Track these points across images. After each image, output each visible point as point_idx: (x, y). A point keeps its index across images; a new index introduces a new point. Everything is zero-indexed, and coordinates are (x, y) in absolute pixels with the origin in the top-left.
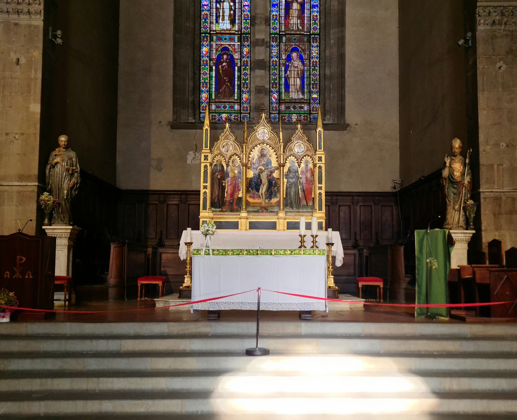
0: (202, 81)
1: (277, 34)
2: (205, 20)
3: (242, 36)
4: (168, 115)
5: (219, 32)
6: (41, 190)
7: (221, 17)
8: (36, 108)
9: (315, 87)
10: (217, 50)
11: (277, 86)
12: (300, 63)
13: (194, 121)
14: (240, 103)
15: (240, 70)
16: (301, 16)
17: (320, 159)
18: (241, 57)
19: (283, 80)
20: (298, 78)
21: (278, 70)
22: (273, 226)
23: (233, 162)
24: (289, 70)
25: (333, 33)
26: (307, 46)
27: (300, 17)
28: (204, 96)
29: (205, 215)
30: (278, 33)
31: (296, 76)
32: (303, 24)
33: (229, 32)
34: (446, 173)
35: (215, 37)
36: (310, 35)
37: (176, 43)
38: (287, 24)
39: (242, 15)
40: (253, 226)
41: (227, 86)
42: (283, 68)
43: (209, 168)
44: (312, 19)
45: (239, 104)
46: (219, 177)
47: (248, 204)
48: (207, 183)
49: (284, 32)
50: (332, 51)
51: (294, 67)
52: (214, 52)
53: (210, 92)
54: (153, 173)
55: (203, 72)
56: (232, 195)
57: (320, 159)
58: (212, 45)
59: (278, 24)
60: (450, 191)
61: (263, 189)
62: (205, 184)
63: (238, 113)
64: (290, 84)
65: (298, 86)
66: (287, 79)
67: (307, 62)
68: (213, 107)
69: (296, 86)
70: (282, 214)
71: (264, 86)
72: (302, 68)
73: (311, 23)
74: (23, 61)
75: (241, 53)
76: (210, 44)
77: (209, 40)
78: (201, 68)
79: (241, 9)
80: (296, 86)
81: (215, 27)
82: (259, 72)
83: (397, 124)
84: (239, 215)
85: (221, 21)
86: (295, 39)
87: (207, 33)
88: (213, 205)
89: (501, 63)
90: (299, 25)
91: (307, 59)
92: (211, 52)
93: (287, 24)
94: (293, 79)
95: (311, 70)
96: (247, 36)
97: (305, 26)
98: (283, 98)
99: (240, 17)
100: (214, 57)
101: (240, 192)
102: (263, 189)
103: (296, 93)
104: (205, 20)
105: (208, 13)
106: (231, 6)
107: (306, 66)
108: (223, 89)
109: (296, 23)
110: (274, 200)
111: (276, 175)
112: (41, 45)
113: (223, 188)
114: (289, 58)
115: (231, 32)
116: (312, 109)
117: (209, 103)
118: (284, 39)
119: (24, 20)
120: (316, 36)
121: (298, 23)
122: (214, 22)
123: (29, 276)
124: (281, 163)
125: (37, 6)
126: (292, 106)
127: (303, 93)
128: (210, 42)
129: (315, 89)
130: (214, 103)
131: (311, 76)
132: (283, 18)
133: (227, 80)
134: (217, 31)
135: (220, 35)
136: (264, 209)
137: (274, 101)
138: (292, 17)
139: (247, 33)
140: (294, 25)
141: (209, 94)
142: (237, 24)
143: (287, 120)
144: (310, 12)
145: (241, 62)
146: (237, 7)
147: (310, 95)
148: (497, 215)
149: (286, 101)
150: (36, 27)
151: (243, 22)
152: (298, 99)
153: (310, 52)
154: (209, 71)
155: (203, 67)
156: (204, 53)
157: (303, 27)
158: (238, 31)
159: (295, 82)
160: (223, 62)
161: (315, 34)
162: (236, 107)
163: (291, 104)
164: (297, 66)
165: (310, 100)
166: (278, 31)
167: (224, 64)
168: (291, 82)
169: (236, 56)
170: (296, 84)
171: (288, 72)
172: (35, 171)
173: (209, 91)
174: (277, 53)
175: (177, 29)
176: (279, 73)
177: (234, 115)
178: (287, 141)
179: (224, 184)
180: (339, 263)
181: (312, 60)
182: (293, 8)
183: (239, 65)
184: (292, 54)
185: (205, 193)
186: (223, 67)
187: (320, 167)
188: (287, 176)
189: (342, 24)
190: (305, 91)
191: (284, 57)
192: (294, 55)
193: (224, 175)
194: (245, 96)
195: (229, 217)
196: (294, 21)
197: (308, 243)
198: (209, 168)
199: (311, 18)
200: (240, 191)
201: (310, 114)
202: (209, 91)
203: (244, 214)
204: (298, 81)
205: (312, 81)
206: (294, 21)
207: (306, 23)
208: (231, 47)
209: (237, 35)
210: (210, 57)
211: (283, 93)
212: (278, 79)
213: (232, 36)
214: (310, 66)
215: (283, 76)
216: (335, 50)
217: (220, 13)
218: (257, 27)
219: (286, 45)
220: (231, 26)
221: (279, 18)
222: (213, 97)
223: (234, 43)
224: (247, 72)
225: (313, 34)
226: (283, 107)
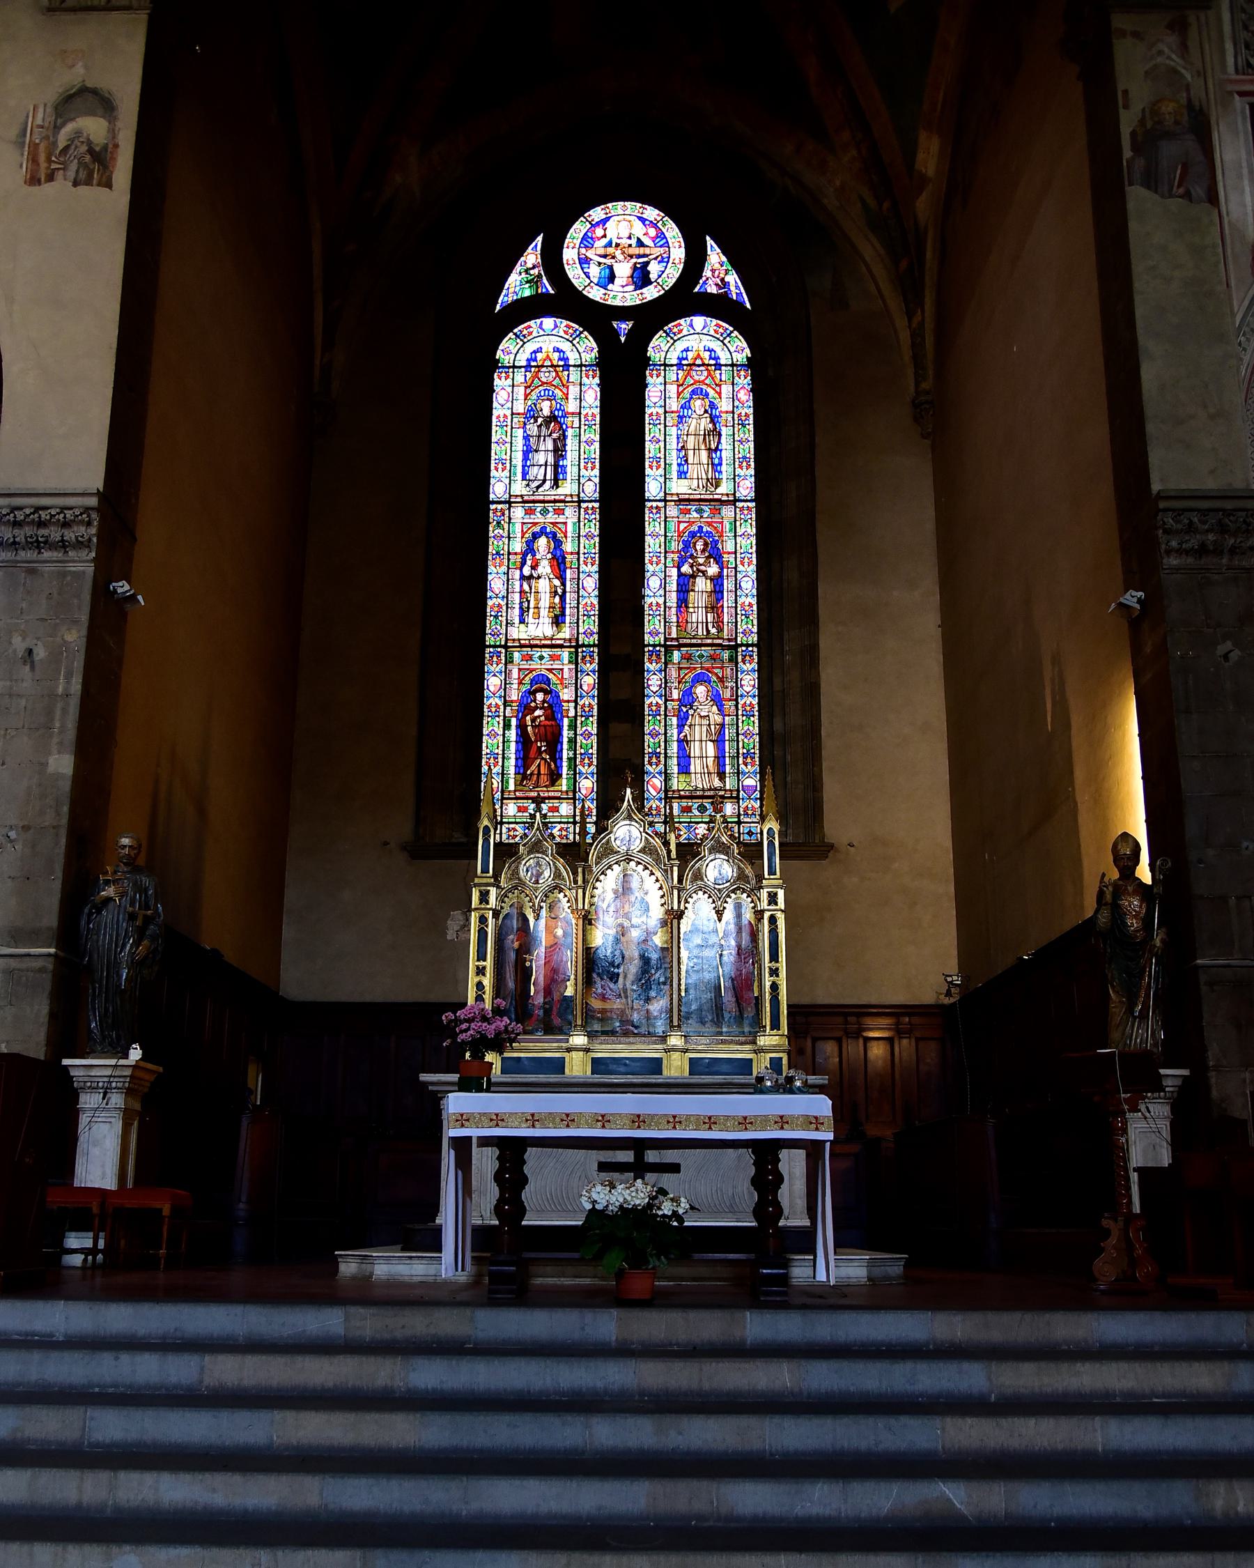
0: (485, 751)
1: (660, 645)
2: (496, 617)
3: (580, 650)
5: (527, 642)
7: (531, 611)
9: (749, 760)
10: (520, 683)
11: (659, 761)
12: (715, 708)
13: (463, 840)
15: (573, 727)
16: (715, 607)
17: (773, 899)
19: (675, 746)
20: (710, 741)
21: (663, 724)
23: (551, 908)
24: (688, 723)
26: (729, 669)
27: (712, 608)
30: (662, 642)
31: (704, 738)
32: (719, 624)
33: (549, 642)
35: (517, 656)
36: (737, 646)
39: (581, 606)
41: (543, 762)
42: (675, 720)
43: (491, 921)
44: (739, 612)
45: (572, 801)
46: (516, 945)
47: (588, 1014)
48: (485, 960)
49: (677, 639)
51: (701, 717)
52: (515, 686)
55: (487, 732)
56: (548, 991)
57: (773, 899)
58: (510, 671)
59: (662, 624)
62: (482, 963)
63: (568, 823)
64: (692, 755)
65: (710, 761)
66: (683, 742)
67: (729, 706)
69: (705, 759)
71: (630, 759)
72: (719, 719)
73: (739, 620)
75: (577, 687)
76: (506, 668)
77: (503, 661)
78: (485, 722)
79: (578, 593)
80: (705, 759)
81: (518, 632)
83: (948, 843)
84: (567, 1041)
85: (530, 619)
86: (701, 656)
87: (500, 646)
90: (710, 626)
91: (730, 700)
92: (507, 686)
94: (697, 743)
95: (740, 724)
96: (592, 649)
97: (725, 627)
98: (675, 788)
99: (576, 610)
100: (514, 695)
101: (568, 983)
103: (706, 775)
104: (496, 617)
105: (503, 603)
106: (556, 587)
107: (729, 715)
108: (533, 767)
109: (704, 621)
114: (688, 699)
115: (553, 642)
116: (744, 811)
118: (676, 656)
120: (750, 649)
121: (709, 621)
122: (517, 620)
124: (672, 908)
125: (83, 529)
126: (695, 804)
127: (722, 776)
128: (506, 664)
129: (749, 767)
130: (514, 801)
131: (741, 737)
132: (674, 611)
133: (543, 749)
134: (522, 642)
135: (529, 649)
137: (654, 793)
138: (694, 608)
139: (592, 643)
140: (700, 625)
141: (502, 781)
142: (567, 625)
143: (685, 839)
144: (736, 596)
145: (576, 708)
146: (568, 589)
147: (739, 780)
149: (682, 793)
150: (79, 575)
151: (581, 621)
152: (710, 789)
153: (736, 683)
154: (501, 730)
155: (490, 719)
156: (492, 689)
157: (720, 630)
158: (570, 640)
159: (703, 752)
160: (536, 708)
161: (747, 645)
163: (694, 801)
164: (708, 716)
165: (738, 791)
166: (662, 639)
167: (538, 713)
168: (695, 750)
169: (566, 694)
170: (704, 755)
171: (686, 727)
173: (503, 774)
174: (660, 686)
176: (666, 730)
177: (559, 827)
179: (528, 964)
181: (741, 702)
182: (696, 590)
183: (572, 713)
184: (696, 687)
185: (480, 986)
186: (533, 720)
187: (773, 920)
190: (727, 771)
191: (675, 695)
192: (700, 690)
196: (698, 616)
198: (491, 921)
199: (739, 609)
200: (569, 980)
201: (739, 823)
202: (503, 774)
203: (579, 1040)
204: (711, 749)
205: (743, 748)
206: (698, 616)
207: (725, 620)
208: (555, 674)
209: (569, 650)
210: (505, 697)
211: (676, 775)
212: (662, 744)
213: (557, 651)
214: (737, 715)
215: (675, 738)
217: (529, 602)
219: (680, 669)
220: (555, 628)
221: (665, 611)
222: (512, 787)
223: (561, 667)
224: (589, 729)
225: (742, 645)
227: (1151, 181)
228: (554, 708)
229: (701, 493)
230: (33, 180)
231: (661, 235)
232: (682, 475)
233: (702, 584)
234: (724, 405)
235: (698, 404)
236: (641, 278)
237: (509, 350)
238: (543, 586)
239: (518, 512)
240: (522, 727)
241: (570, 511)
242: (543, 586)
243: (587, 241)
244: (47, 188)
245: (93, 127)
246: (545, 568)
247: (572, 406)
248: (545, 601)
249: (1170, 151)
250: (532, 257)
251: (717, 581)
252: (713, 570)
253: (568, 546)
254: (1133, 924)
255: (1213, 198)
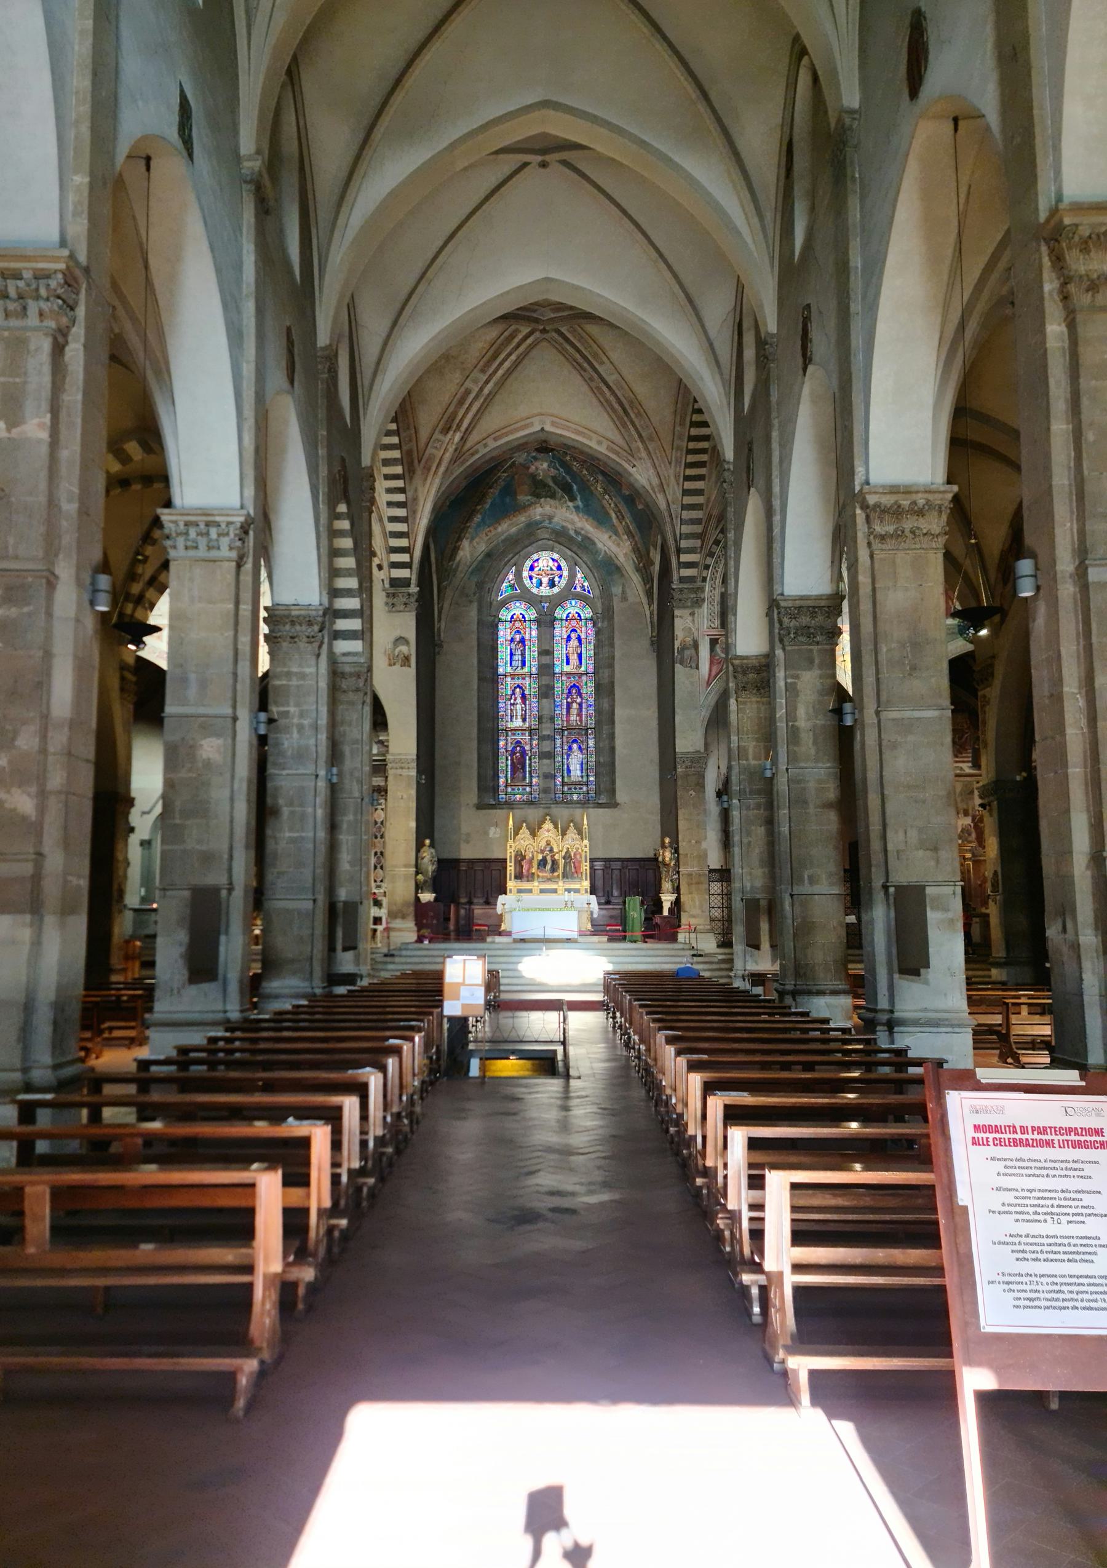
4: (475, 800)
6: (417, 873)
8: (413, 824)
14: (531, 786)
15: (530, 759)
16: (579, 714)
18: (531, 748)
22: (555, 891)
25: (606, 729)
28: (502, 781)
29: (511, 884)
32: (581, 720)
34: (660, 859)
37: (480, 741)
38: (568, 721)
40: (542, 891)
50: (605, 744)
53: (506, 777)
54: (463, 846)
56: (528, 870)
60: (663, 870)
61: (549, 867)
68: (509, 789)
70: (561, 883)
74: (405, 796)
82: (546, 761)
88: (516, 877)
89: (692, 792)
93: (568, 721)
100: (510, 749)
102: (549, 867)
110: (556, 874)
111: (556, 857)
112: (415, 786)
113: (522, 867)
114: (570, 748)
117: (506, 786)
119: (405, 772)
123: (435, 922)
136: (549, 880)
148: (689, 884)
162: (528, 789)
168: (572, 768)
169: (527, 748)
172: (413, 862)
175: (480, 730)
178: (564, 834)
180: (595, 916)
188: (564, 858)
189: (612, 722)
193: (524, 858)
194: (535, 780)
195: (526, 885)
196: (574, 718)
197: (569, 905)
204: (578, 767)
206: (574, 718)
216: (607, 742)
218: (544, 725)
226: (566, 788)
227: (681, 664)
228: (523, 753)
229: (575, 671)
230: (390, 665)
231: (559, 568)
232: (568, 663)
233: (575, 706)
234: (583, 636)
235: (573, 635)
236: (552, 584)
237: (504, 614)
238: (519, 707)
239: (509, 679)
240: (512, 760)
241: (527, 679)
242: (519, 707)
243: (532, 568)
244: (394, 667)
245: (404, 649)
246: (519, 700)
247: (527, 637)
248: (519, 713)
249: (687, 653)
250: (511, 576)
251: (580, 705)
252: (579, 700)
253: (527, 692)
254: (667, 859)
255: (697, 668)
